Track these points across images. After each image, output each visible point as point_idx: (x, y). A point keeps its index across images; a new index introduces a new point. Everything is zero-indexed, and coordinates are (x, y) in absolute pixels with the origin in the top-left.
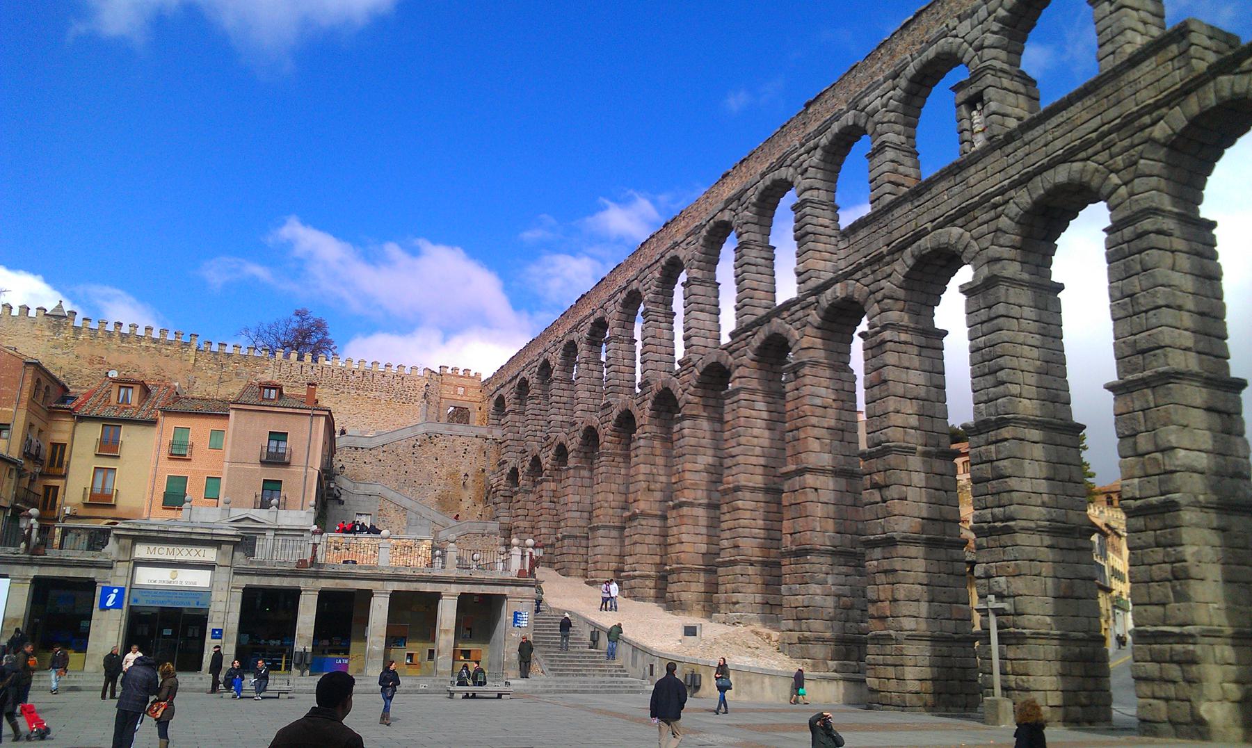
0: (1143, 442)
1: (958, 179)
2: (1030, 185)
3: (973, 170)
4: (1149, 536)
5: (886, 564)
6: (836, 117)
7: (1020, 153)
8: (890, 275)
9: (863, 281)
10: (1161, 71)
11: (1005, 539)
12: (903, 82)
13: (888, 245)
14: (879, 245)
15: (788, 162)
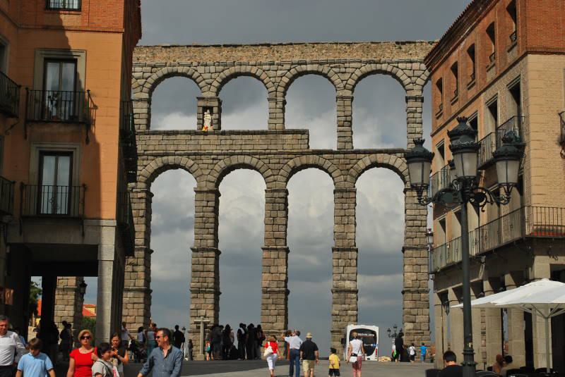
1: (193, 137)
3: (202, 137)
4: (270, 301)
7: (228, 142)
8: (146, 166)
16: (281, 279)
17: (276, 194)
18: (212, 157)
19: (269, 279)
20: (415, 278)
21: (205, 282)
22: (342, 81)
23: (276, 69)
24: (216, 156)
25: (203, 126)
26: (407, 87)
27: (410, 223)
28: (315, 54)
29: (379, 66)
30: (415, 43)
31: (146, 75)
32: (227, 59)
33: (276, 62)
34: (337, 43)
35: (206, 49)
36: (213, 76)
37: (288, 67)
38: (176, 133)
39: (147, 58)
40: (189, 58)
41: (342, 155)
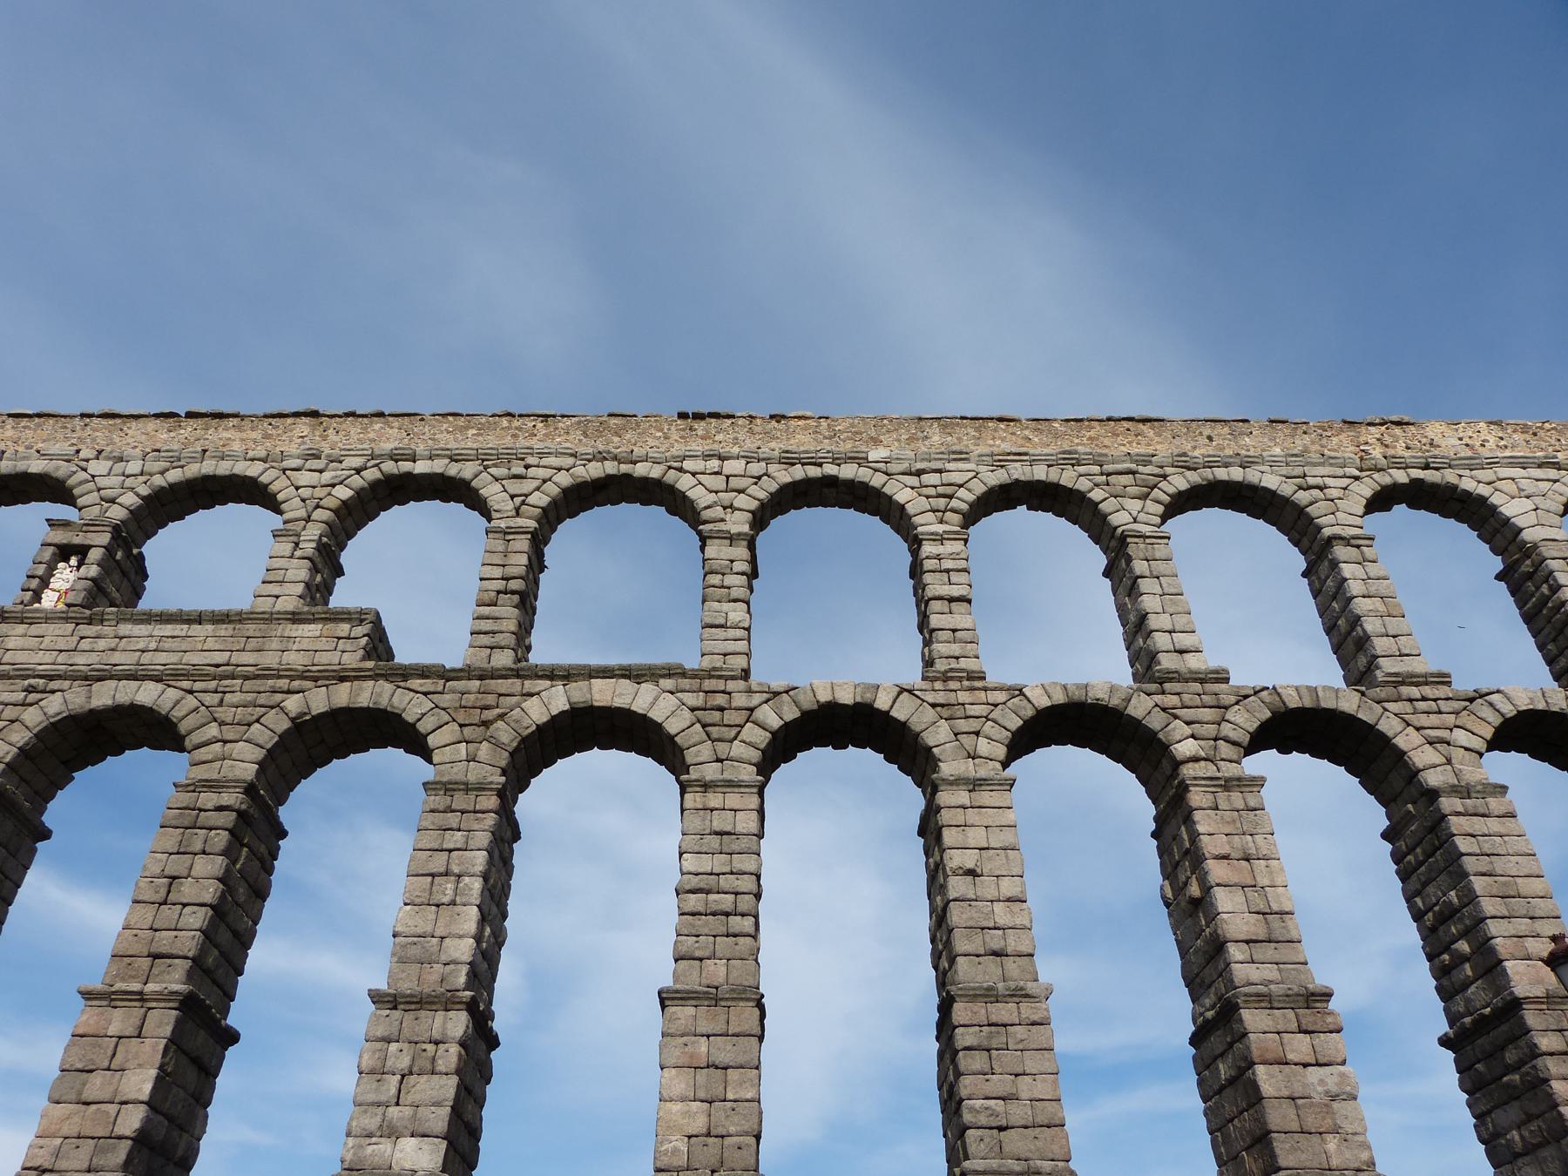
2: (96, 686)
3: (21, 629)
16: (119, 1131)
17: (208, 799)
19: (65, 1131)
20: (699, 1125)
22: (512, 497)
26: (706, 514)
27: (694, 902)
29: (624, 468)
30: (733, 417)
33: (327, 451)
34: (509, 414)
35: (134, 424)
36: (129, 482)
37: (357, 462)
41: (478, 683)
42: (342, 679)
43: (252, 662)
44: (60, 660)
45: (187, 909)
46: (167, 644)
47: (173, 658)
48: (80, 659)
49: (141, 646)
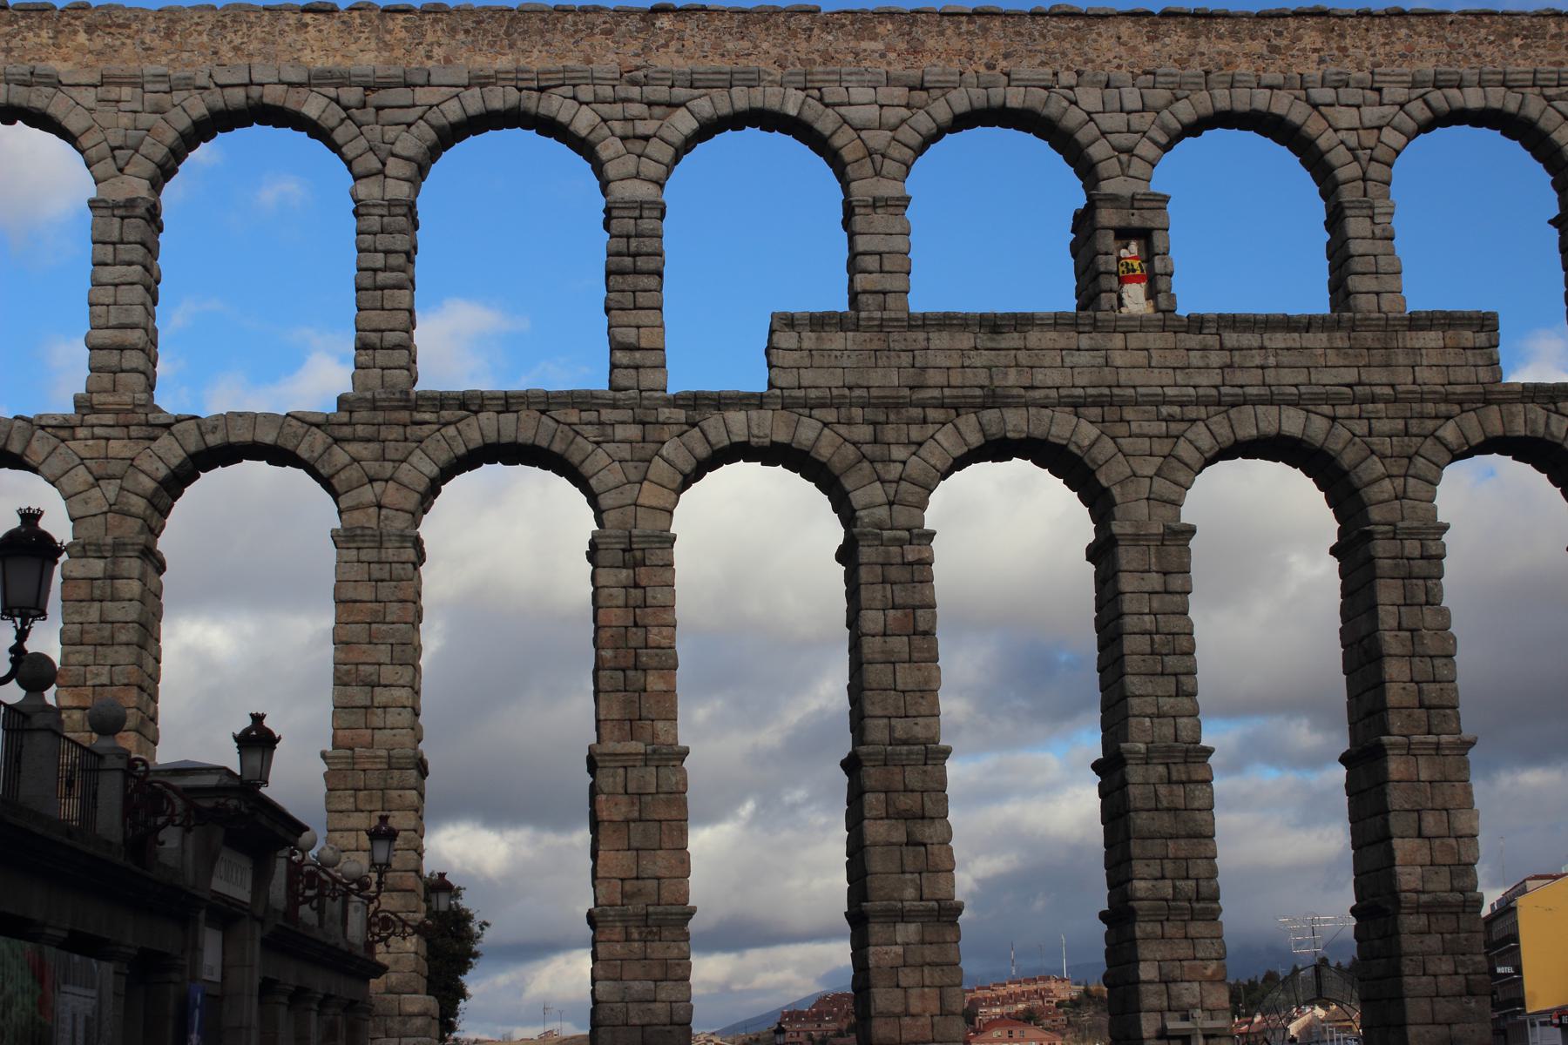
0: (1430, 822)
1: (1085, 341)
2: (1233, 412)
3: (1118, 340)
4: (1433, 941)
5: (930, 953)
6: (753, 80)
7: (1216, 358)
8: (920, 444)
9: (842, 430)
10: (1451, 357)
11: (1196, 928)
12: (943, 113)
13: (911, 388)
14: (887, 379)
15: (585, 93)
17: (1413, 547)
18: (1165, 410)
19: (1419, 860)
21: (1187, 878)
23: (1359, 100)
24: (1176, 410)
25: (1121, 303)
28: (1487, 51)
31: (892, 115)
32: (1182, 63)
35: (1102, 28)
36: (1134, 118)
37: (1400, 94)
38: (1022, 322)
39: (892, 56)
40: (1042, 57)
42: (1487, 402)
43: (1384, 380)
44: (1180, 381)
45: (1438, 662)
46: (1286, 359)
47: (1301, 377)
48: (1202, 379)
49: (1258, 361)
